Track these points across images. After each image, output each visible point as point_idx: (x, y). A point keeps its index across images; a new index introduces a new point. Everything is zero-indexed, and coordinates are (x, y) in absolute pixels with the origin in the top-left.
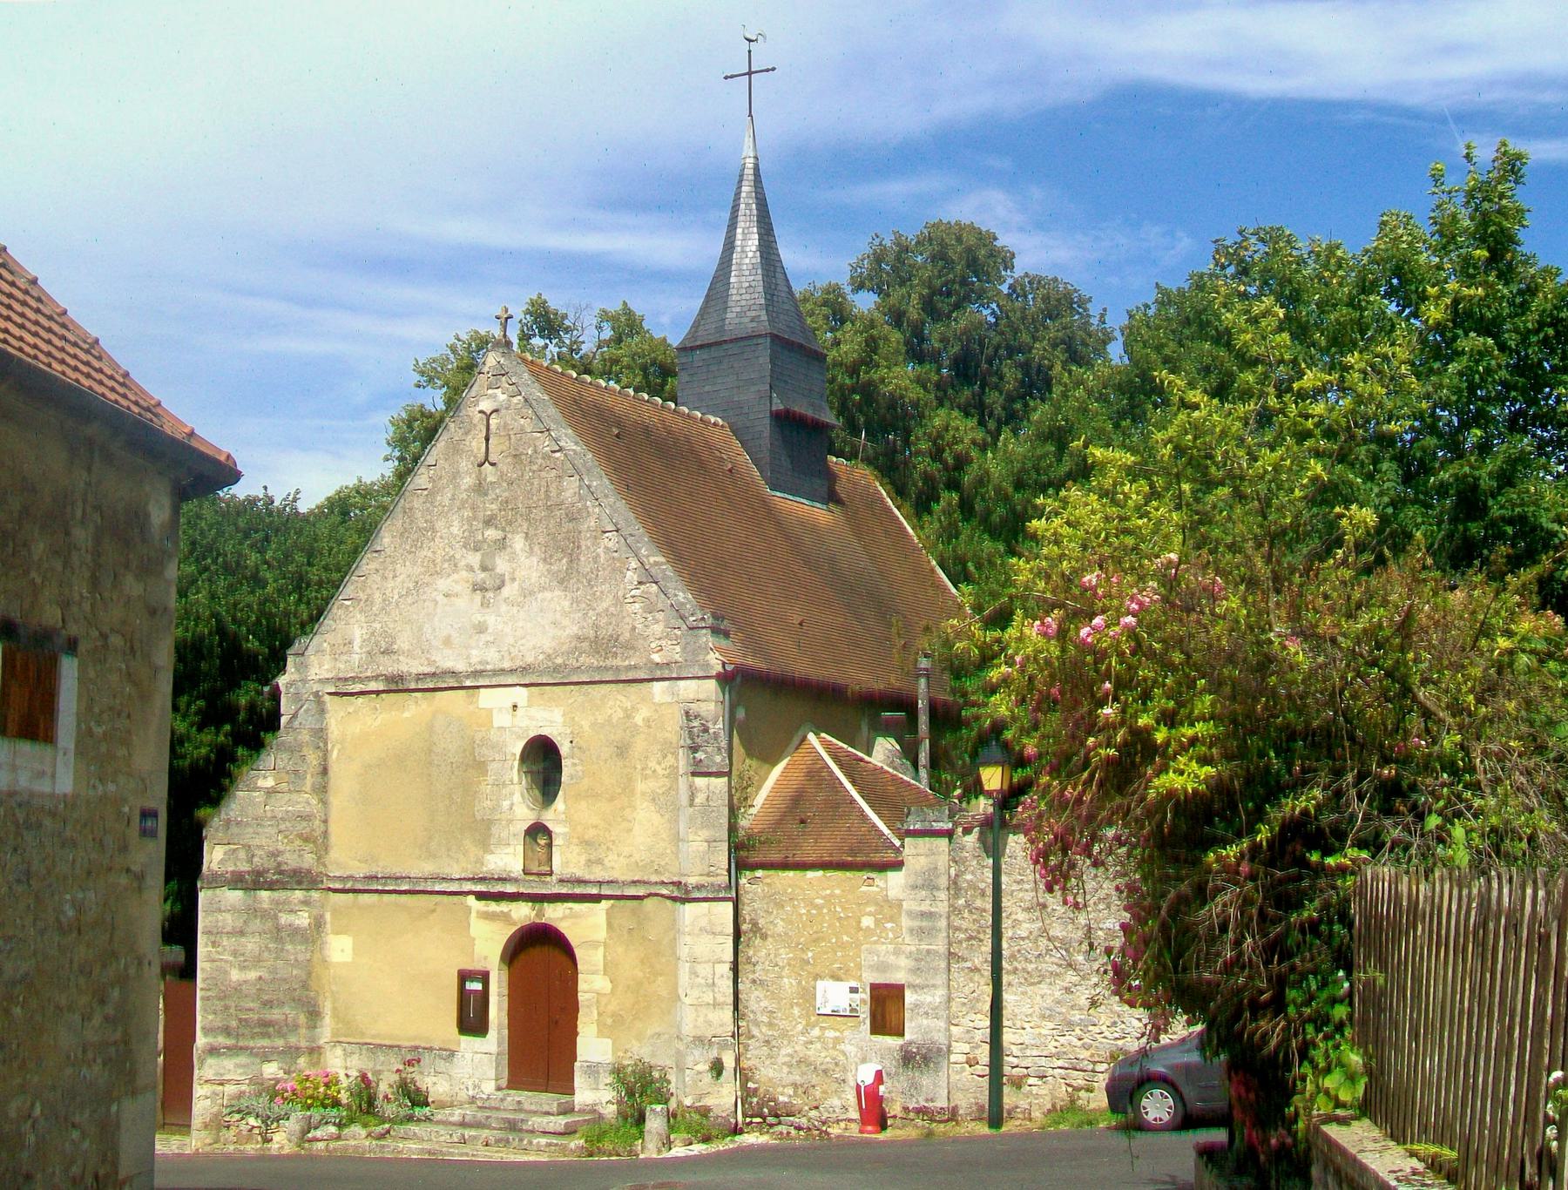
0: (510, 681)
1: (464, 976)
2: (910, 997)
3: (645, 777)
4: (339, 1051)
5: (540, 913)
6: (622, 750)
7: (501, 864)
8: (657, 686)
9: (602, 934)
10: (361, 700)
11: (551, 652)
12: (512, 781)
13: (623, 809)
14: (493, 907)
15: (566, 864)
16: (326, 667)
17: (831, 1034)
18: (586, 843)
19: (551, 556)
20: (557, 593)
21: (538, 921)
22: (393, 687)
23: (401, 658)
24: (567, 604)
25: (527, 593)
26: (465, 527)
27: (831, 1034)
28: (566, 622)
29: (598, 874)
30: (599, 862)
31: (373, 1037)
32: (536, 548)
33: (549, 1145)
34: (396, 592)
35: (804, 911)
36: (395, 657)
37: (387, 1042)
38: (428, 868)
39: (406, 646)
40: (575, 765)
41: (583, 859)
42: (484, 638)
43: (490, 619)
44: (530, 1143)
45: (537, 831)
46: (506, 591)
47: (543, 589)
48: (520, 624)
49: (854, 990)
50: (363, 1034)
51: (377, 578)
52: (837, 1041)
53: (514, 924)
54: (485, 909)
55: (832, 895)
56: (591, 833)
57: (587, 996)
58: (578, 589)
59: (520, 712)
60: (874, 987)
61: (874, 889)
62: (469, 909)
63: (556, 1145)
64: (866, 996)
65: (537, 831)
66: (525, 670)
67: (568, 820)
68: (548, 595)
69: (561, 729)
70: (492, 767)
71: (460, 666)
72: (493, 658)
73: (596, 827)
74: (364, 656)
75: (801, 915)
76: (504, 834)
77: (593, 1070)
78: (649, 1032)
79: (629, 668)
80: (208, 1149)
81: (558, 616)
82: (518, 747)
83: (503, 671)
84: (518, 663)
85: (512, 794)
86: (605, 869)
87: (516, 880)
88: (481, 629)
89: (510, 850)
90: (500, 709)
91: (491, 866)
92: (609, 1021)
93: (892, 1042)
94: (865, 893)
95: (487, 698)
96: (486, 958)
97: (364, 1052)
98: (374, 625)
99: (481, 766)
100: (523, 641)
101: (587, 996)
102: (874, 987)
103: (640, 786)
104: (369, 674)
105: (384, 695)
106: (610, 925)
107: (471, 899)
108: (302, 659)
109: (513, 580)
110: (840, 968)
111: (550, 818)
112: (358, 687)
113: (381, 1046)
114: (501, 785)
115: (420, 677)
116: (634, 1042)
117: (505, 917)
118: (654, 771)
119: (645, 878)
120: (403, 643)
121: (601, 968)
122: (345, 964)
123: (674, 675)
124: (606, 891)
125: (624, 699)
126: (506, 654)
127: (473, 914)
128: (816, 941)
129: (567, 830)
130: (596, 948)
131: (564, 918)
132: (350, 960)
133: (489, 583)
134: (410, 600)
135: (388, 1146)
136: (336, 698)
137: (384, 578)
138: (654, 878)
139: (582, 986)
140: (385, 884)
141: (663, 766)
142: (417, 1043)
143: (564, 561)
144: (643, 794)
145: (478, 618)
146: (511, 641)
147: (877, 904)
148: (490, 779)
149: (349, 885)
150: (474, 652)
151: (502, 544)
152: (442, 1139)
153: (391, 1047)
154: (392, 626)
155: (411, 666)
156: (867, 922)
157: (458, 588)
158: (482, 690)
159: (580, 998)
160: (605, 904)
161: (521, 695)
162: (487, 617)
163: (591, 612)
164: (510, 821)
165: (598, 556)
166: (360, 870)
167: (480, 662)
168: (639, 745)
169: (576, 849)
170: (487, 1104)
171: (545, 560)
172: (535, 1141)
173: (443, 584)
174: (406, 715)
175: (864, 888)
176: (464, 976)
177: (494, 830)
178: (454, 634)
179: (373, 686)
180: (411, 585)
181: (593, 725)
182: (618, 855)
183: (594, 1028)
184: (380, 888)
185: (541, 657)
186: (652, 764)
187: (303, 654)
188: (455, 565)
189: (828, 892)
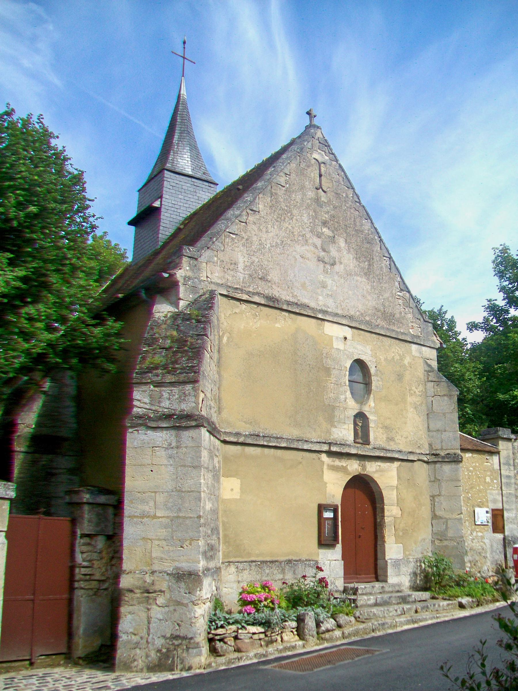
0: (344, 322)
1: (321, 508)
2: (506, 514)
3: (411, 395)
4: (232, 569)
5: (364, 467)
6: (400, 377)
7: (341, 435)
8: (414, 347)
9: (395, 482)
10: (244, 306)
11: (363, 312)
12: (345, 383)
13: (402, 410)
14: (338, 462)
15: (375, 439)
16: (217, 274)
17: (480, 534)
18: (386, 428)
19: (359, 258)
20: (364, 280)
21: (362, 473)
22: (271, 304)
23: (273, 286)
24: (369, 287)
25: (349, 274)
26: (311, 221)
27: (480, 534)
28: (369, 298)
29: (392, 446)
30: (392, 439)
31: (258, 555)
32: (352, 250)
33: (448, 605)
34: (268, 242)
35: (466, 473)
36: (270, 284)
37: (268, 559)
38: (295, 433)
39: (276, 279)
40: (378, 381)
41: (384, 436)
42: (326, 291)
43: (329, 282)
44: (439, 606)
45: (361, 416)
46: (337, 268)
47: (356, 275)
48: (346, 290)
49: (487, 512)
50: (249, 554)
51: (255, 228)
52: (482, 537)
53: (349, 474)
54: (332, 463)
55: (476, 466)
56: (388, 422)
57: (390, 519)
58: (374, 282)
59: (348, 342)
60: (493, 510)
61: (489, 464)
62: (323, 463)
63: (452, 604)
64: (489, 515)
65: (361, 416)
66: (351, 318)
67: (376, 413)
68: (359, 278)
69: (371, 358)
70: (334, 372)
71: (312, 305)
72: (331, 306)
73: (390, 419)
74: (247, 276)
75: (465, 475)
76: (342, 417)
77: (397, 564)
78: (420, 538)
79: (403, 333)
80: (123, 674)
81: (365, 292)
82: (348, 364)
83: (336, 315)
84: (346, 313)
85: (346, 392)
86: (395, 444)
87: (349, 446)
88: (324, 286)
89: (346, 426)
90: (337, 338)
91: (336, 436)
92: (401, 534)
93: (500, 536)
94: (486, 465)
95: (330, 329)
96: (334, 496)
97: (253, 568)
98: (254, 258)
99: (328, 371)
100: (348, 301)
101: (390, 519)
102: (493, 510)
103: (409, 399)
104: (251, 290)
105: (262, 308)
106: (399, 478)
107: (324, 457)
108: (196, 262)
109: (341, 263)
110: (480, 502)
111: (366, 410)
112: (245, 297)
113: (263, 562)
114: (338, 384)
115: (289, 303)
116: (413, 545)
117: (344, 469)
118: (415, 392)
119: (414, 451)
120: (274, 275)
121: (396, 502)
122: (235, 500)
123: (422, 343)
124: (396, 456)
125: (399, 349)
126: (339, 305)
127: (325, 467)
128: (472, 488)
129: (376, 418)
130: (393, 490)
131: (377, 471)
132: (238, 497)
133: (326, 260)
134: (278, 251)
135: (387, 623)
136: (225, 299)
137: (260, 230)
138: (418, 451)
139: (386, 513)
140: (269, 441)
141: (419, 390)
142: (290, 557)
143: (366, 263)
144: (411, 403)
145: (321, 277)
146: (342, 299)
147: (491, 471)
148: (333, 379)
149: (241, 440)
150: (321, 298)
151: (333, 240)
152: (391, 614)
153: (272, 562)
154: (266, 263)
155: (284, 295)
156: (488, 479)
157: (309, 255)
158: (326, 323)
159: (386, 521)
160: (396, 464)
161: (348, 332)
162: (327, 280)
163: (381, 297)
164: (345, 409)
165: (382, 267)
166: (246, 429)
167: (324, 305)
168: (407, 377)
169: (381, 431)
170: (364, 592)
171: (356, 258)
172: (441, 604)
173: (300, 249)
174: (277, 325)
175: (486, 464)
176: (321, 508)
177: (337, 413)
178: (308, 283)
179: (256, 299)
180: (279, 242)
181: (386, 359)
182: (402, 436)
183: (393, 538)
184: (265, 443)
185: (358, 313)
186: (414, 388)
187: (196, 259)
188: (306, 240)
189: (474, 464)
